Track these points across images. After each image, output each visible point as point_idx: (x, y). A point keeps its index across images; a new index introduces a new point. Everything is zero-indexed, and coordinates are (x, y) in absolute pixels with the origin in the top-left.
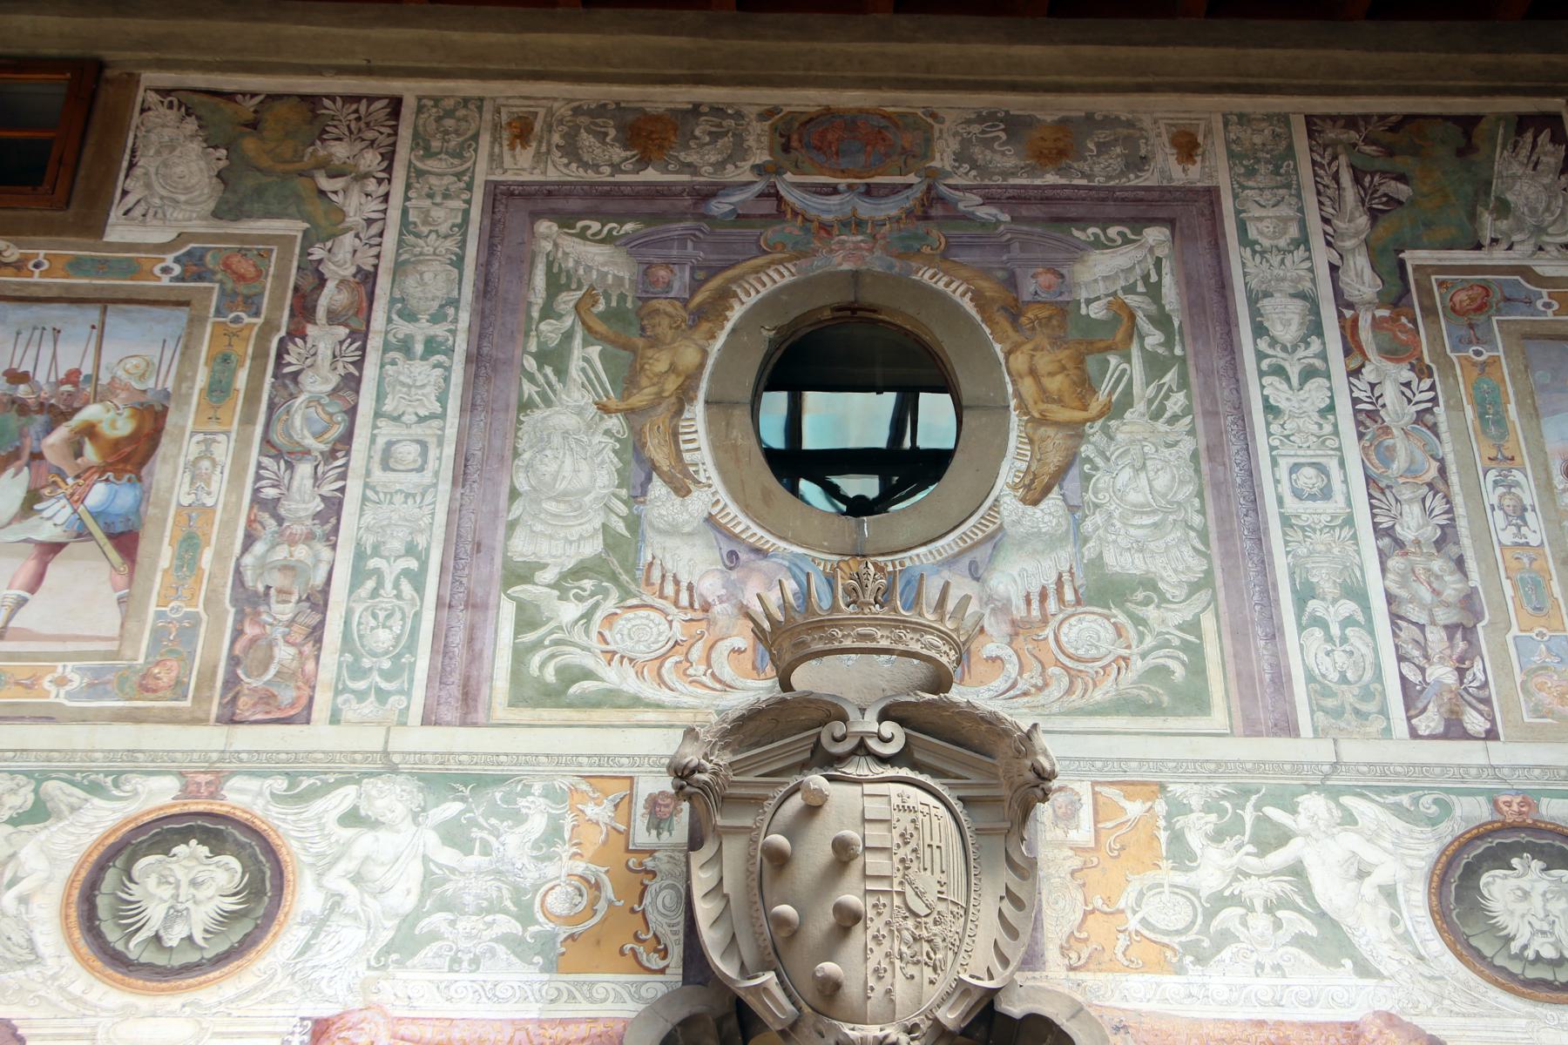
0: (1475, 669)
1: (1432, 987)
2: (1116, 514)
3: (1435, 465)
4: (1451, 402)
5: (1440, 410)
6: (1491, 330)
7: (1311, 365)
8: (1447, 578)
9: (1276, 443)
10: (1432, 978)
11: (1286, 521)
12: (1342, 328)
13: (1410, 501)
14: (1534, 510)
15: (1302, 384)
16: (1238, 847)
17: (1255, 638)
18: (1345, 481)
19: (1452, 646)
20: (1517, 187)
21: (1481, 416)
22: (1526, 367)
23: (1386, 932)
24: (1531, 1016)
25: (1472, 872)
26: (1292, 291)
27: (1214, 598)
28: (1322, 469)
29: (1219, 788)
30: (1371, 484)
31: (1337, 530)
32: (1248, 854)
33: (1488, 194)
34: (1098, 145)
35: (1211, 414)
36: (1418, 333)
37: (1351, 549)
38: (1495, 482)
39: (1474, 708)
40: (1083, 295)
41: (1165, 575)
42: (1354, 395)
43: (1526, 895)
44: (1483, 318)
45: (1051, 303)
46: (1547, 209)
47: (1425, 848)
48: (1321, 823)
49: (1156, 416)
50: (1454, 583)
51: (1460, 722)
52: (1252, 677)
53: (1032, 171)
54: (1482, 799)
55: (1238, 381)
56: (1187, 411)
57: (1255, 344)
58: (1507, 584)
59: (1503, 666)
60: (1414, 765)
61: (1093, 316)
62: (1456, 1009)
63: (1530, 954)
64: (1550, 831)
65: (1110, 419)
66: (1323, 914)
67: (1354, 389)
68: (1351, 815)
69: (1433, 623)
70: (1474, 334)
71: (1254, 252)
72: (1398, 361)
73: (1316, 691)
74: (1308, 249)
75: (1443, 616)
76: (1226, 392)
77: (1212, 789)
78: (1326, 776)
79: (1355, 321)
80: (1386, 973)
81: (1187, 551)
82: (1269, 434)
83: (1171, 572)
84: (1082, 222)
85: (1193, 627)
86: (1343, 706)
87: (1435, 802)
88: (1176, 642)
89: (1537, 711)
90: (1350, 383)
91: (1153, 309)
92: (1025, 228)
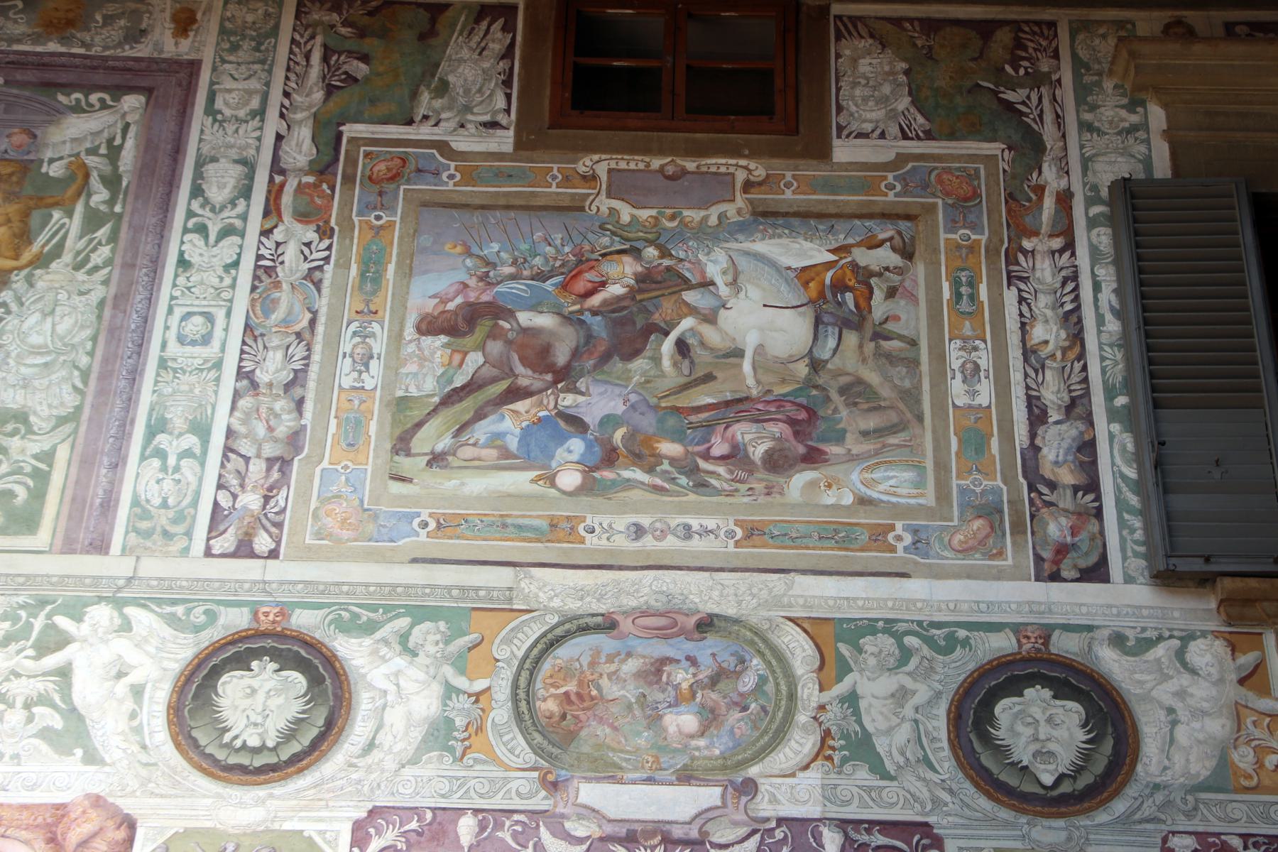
0: (279, 497)
1: (144, 772)
2: (13, 355)
3: (308, 316)
4: (341, 261)
5: (329, 269)
6: (396, 198)
7: (231, 225)
8: (285, 417)
9: (177, 293)
10: (147, 765)
11: (163, 363)
12: (269, 192)
13: (276, 348)
14: (379, 358)
15: (217, 242)
16: (19, 652)
17: (99, 467)
18: (226, 330)
19: (267, 477)
20: (460, 70)
21: (362, 275)
22: (415, 231)
23: (123, 725)
24: (219, 796)
25: (216, 672)
26: (236, 157)
27: (76, 431)
28: (209, 318)
29: (21, 600)
30: (248, 330)
31: (205, 373)
32: (26, 657)
33: (433, 76)
34: (105, 18)
35: (129, 266)
36: (333, 199)
37: (210, 392)
38: (355, 334)
39: (267, 531)
40: (49, 154)
41: (38, 408)
42: (260, 252)
43: (254, 691)
44: (393, 186)
45: (16, 161)
46: (480, 91)
47: (184, 650)
48: (100, 630)
49: (77, 267)
50: (290, 420)
51: (250, 542)
52: (84, 501)
53: (36, 40)
54: (246, 610)
55: (162, 237)
56: (109, 262)
57: (189, 204)
58: (333, 422)
59: (304, 496)
60: (198, 580)
61: (51, 174)
62: (157, 791)
63: (238, 743)
64: (293, 637)
65: (37, 268)
66: (74, 710)
67: (261, 247)
68: (129, 623)
69: (258, 456)
70: (382, 201)
71: (215, 120)
72: (307, 223)
73: (136, 515)
74: (262, 120)
75: (269, 450)
76: (149, 247)
77: (15, 599)
78: (119, 589)
79: (282, 186)
80: (108, 760)
81: (67, 388)
82: (174, 285)
83: (45, 407)
84: (68, 88)
85: (48, 457)
86: (154, 529)
87: (206, 612)
88: (28, 469)
89: (319, 535)
90: (260, 241)
91: (107, 169)
92: (15, 91)
